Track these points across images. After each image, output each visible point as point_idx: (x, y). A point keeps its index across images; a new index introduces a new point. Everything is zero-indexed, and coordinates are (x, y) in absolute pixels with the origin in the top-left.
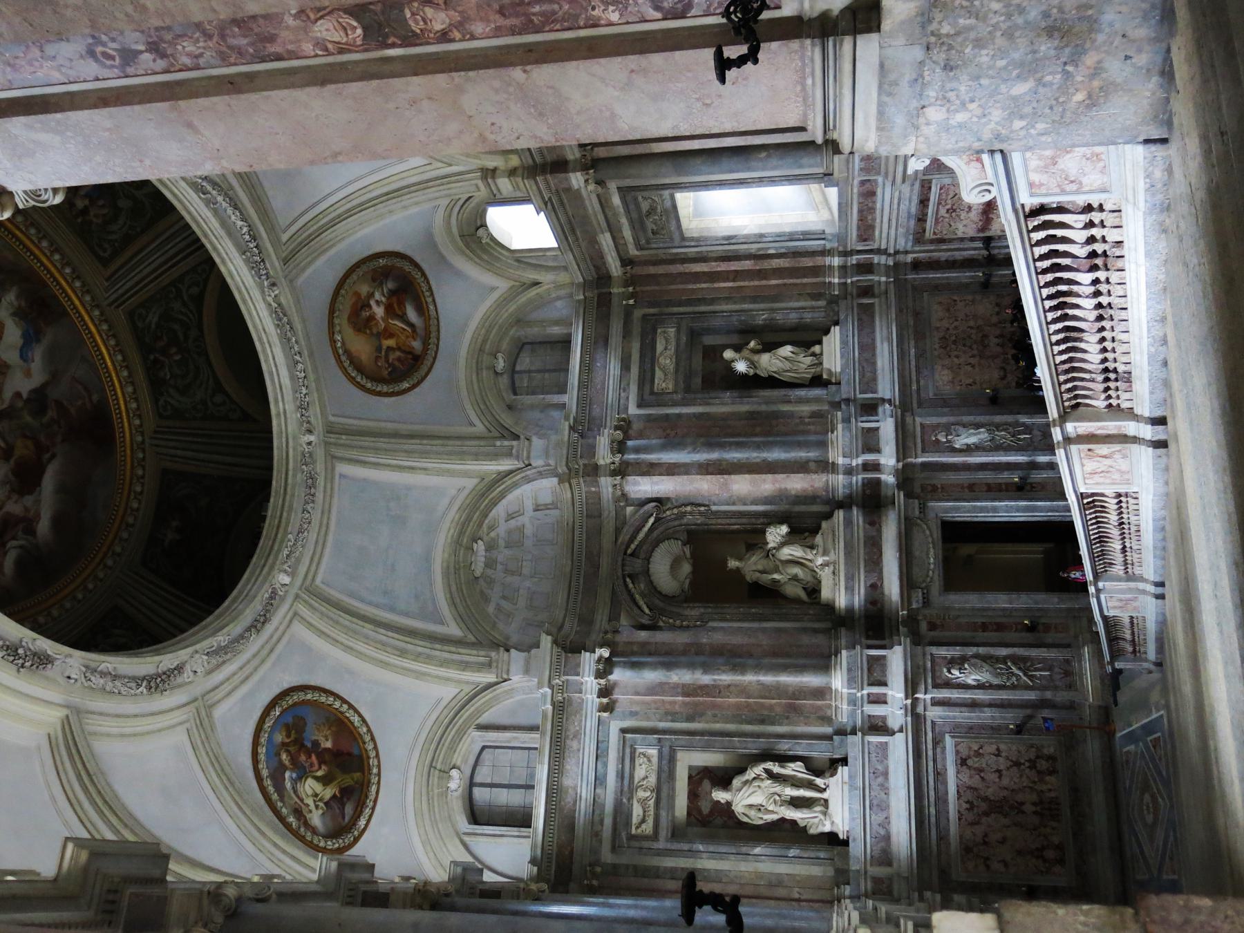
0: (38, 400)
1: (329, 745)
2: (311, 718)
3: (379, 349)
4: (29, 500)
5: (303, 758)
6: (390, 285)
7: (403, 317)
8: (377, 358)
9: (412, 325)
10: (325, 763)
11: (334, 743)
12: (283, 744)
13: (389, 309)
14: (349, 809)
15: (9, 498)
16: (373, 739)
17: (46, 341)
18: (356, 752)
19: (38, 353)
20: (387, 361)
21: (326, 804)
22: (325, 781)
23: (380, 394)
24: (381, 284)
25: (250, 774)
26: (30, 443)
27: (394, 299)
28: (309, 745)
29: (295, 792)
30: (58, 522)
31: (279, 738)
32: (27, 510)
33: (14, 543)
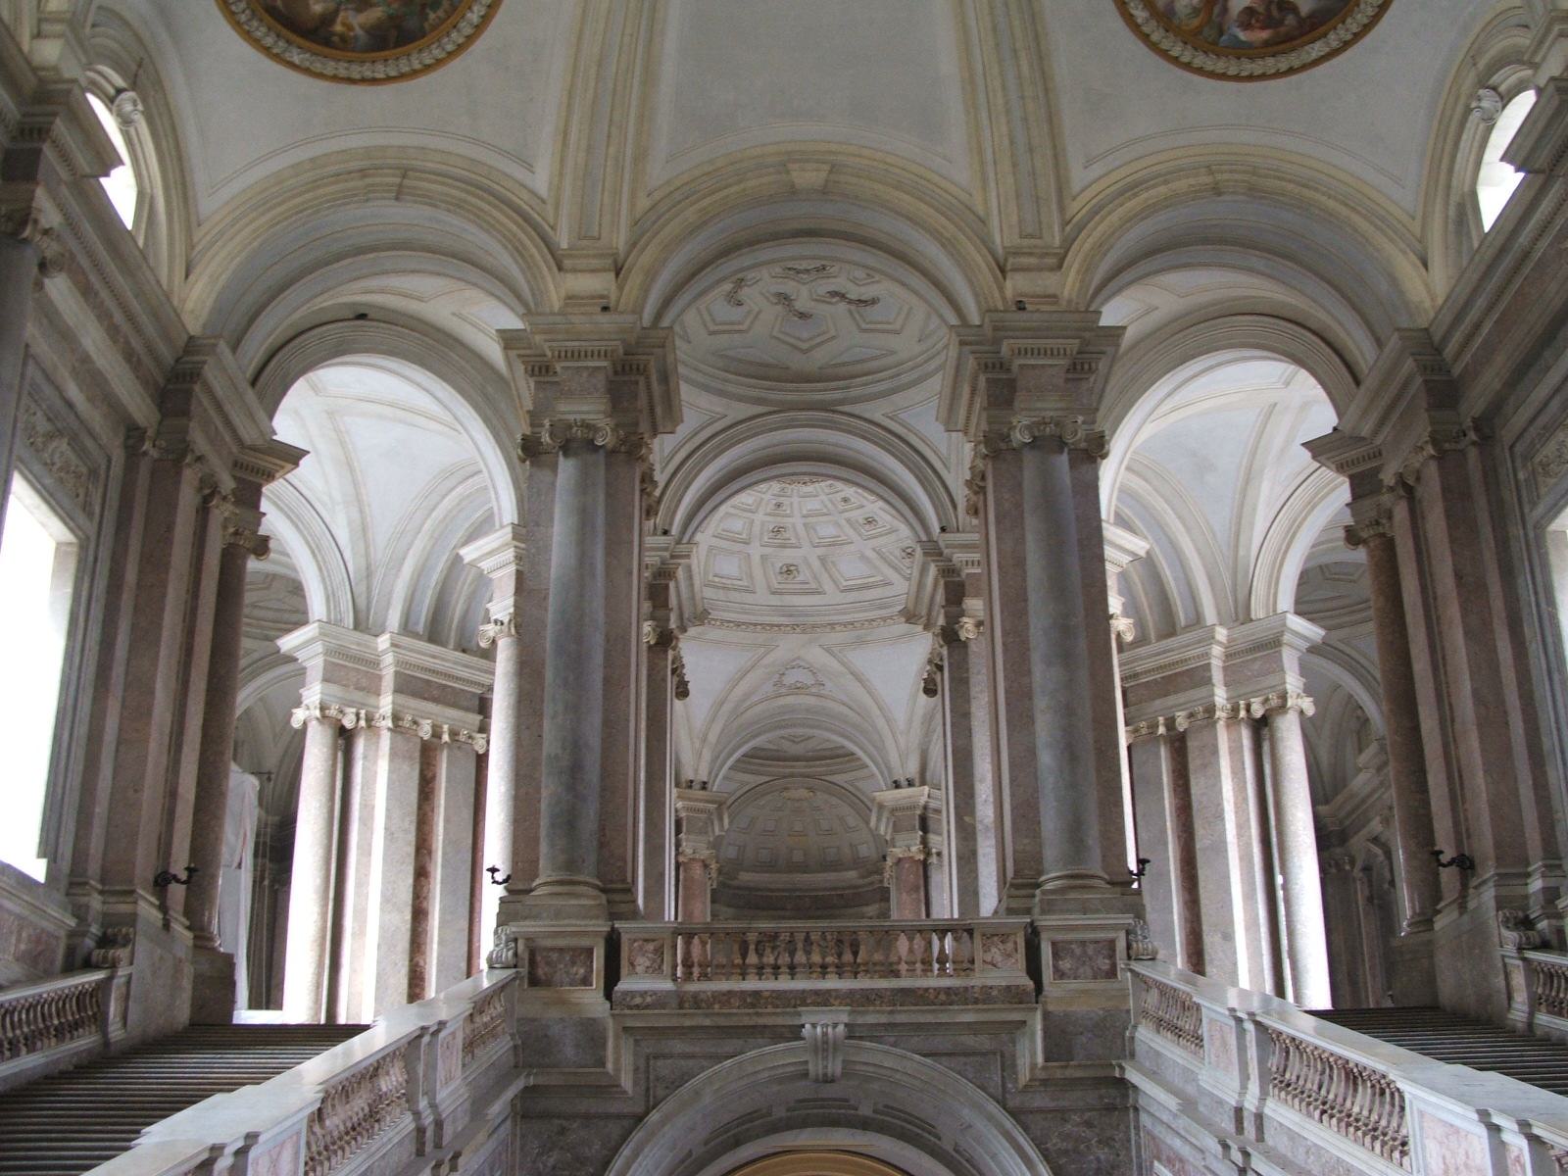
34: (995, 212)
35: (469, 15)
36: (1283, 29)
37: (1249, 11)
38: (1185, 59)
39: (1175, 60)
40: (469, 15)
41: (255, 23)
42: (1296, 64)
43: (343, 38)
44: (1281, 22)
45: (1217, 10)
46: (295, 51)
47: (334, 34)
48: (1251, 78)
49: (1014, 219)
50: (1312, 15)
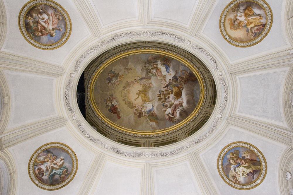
0: (175, 79)
1: (248, 158)
2: (241, 150)
3: (247, 30)
4: (180, 100)
5: (239, 161)
6: (242, 8)
7: (254, 14)
8: (247, 34)
9: (259, 15)
10: (247, 163)
11: (250, 157)
12: (231, 158)
13: (246, 15)
14: (256, 176)
15: (175, 101)
16: (263, 157)
17: (171, 66)
18: (258, 160)
19: (171, 69)
20: (252, 32)
21: (247, 174)
22: (248, 167)
23: (251, 45)
24: (238, 10)
25: (216, 167)
26: (177, 88)
27: (247, 11)
28: (241, 158)
29: (235, 171)
30: (188, 102)
31: (229, 156)
32: (180, 102)
33: (178, 110)
34: (5, 135)
35: (32, 41)
36: (39, 175)
37: (41, 169)
38: (31, 161)
39: (31, 159)
40: (32, 41)
41: (34, 3)
42: (33, 180)
43: (27, 18)
44: (40, 175)
45: (40, 164)
46: (27, 9)
47: (29, 16)
48: (29, 173)
49: (6, 139)
50: (42, 179)
